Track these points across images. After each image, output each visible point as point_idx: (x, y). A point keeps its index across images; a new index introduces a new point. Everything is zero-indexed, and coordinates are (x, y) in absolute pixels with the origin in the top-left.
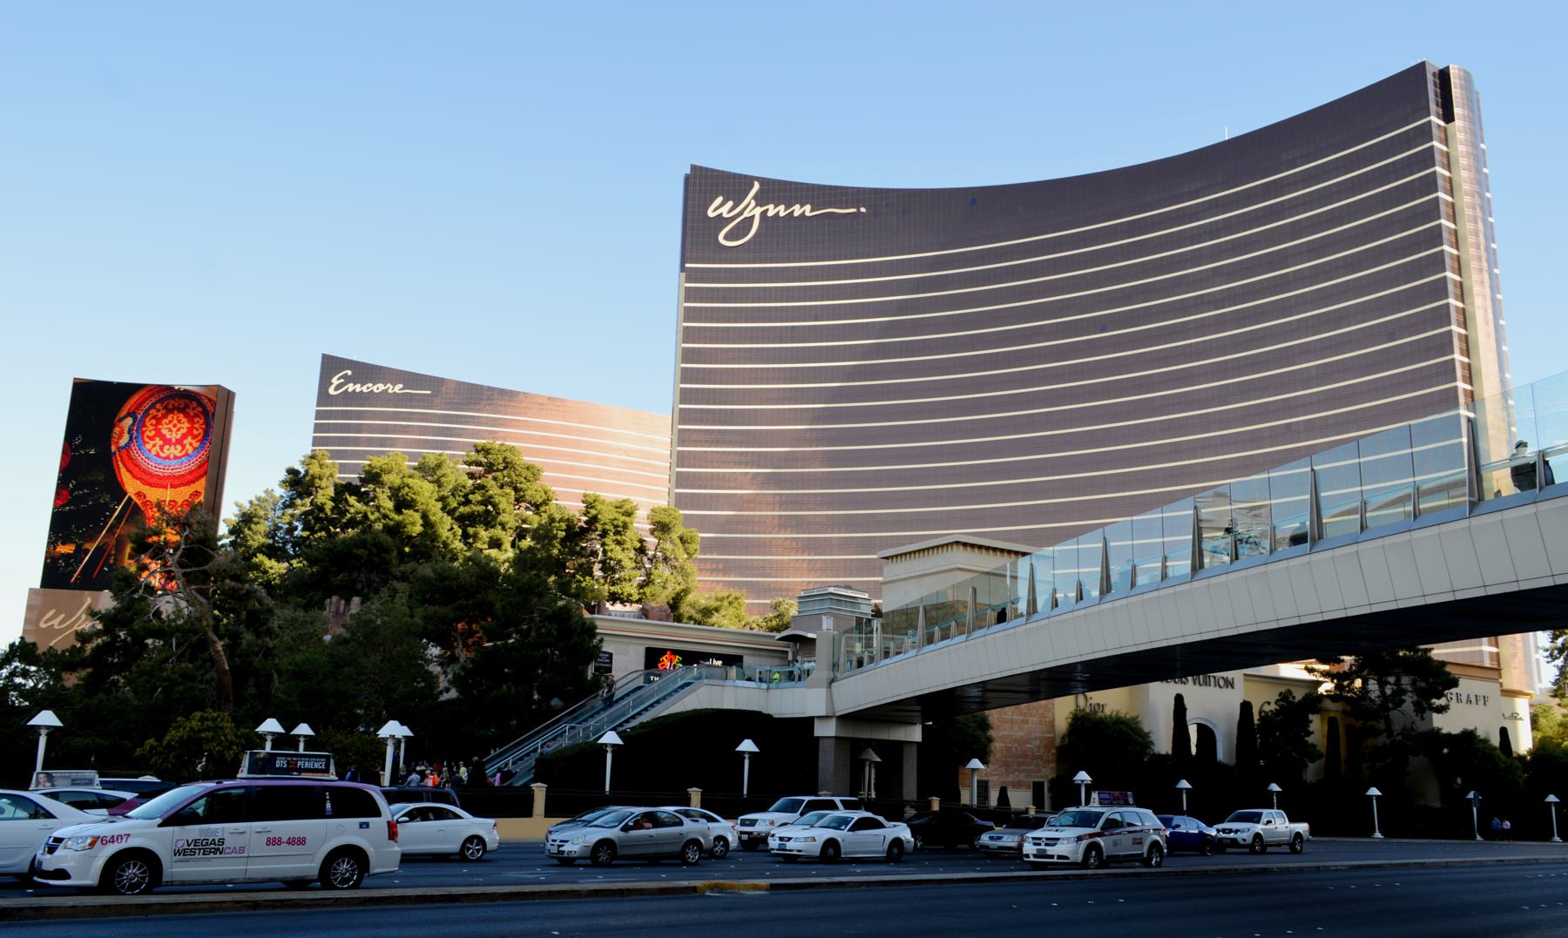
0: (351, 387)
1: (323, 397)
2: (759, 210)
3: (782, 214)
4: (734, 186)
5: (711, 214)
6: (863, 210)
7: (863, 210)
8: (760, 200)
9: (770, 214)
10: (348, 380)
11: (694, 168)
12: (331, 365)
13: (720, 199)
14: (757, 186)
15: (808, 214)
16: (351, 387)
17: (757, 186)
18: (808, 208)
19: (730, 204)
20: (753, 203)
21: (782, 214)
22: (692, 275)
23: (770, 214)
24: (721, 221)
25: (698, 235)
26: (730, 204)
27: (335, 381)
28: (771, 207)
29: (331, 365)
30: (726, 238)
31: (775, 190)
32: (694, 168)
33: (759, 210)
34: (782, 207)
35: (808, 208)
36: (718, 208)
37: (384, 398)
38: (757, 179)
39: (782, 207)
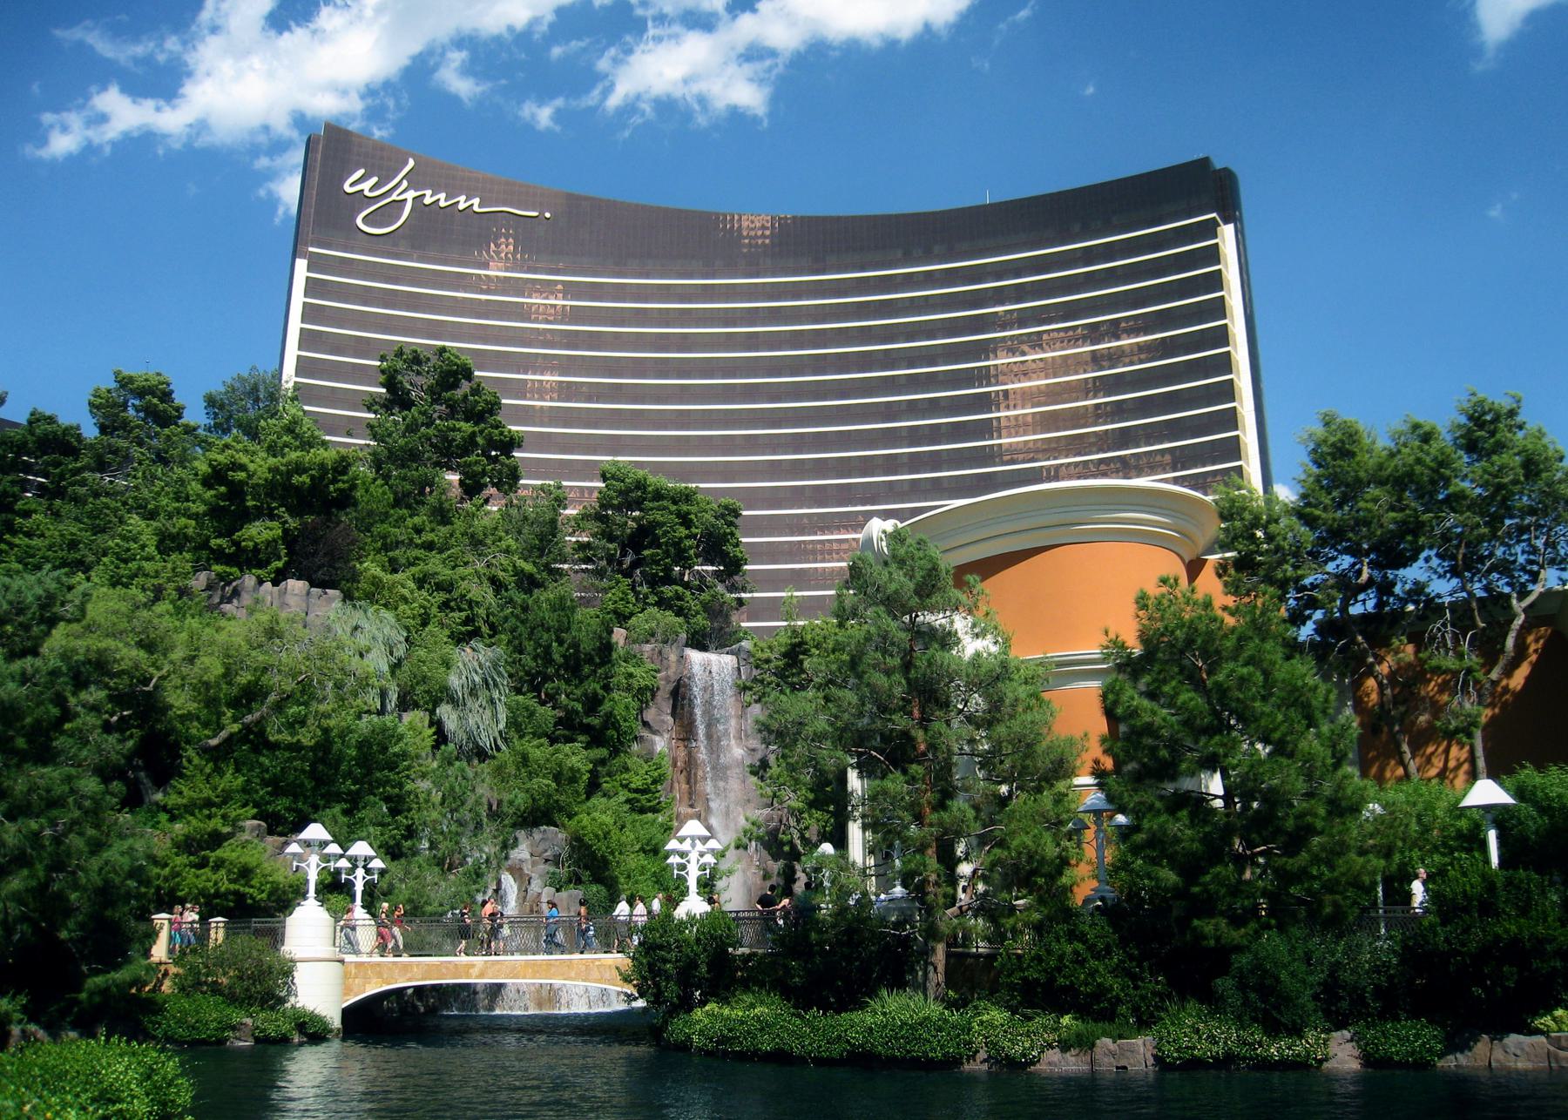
2: (411, 195)
3: (442, 204)
7: (548, 215)
8: (414, 180)
9: (428, 201)
13: (361, 172)
14: (411, 163)
15: (476, 208)
17: (411, 163)
18: (476, 201)
19: (374, 180)
20: (405, 184)
22: (315, 264)
24: (360, 199)
26: (374, 180)
33: (411, 195)
34: (442, 196)
35: (476, 201)
39: (442, 196)
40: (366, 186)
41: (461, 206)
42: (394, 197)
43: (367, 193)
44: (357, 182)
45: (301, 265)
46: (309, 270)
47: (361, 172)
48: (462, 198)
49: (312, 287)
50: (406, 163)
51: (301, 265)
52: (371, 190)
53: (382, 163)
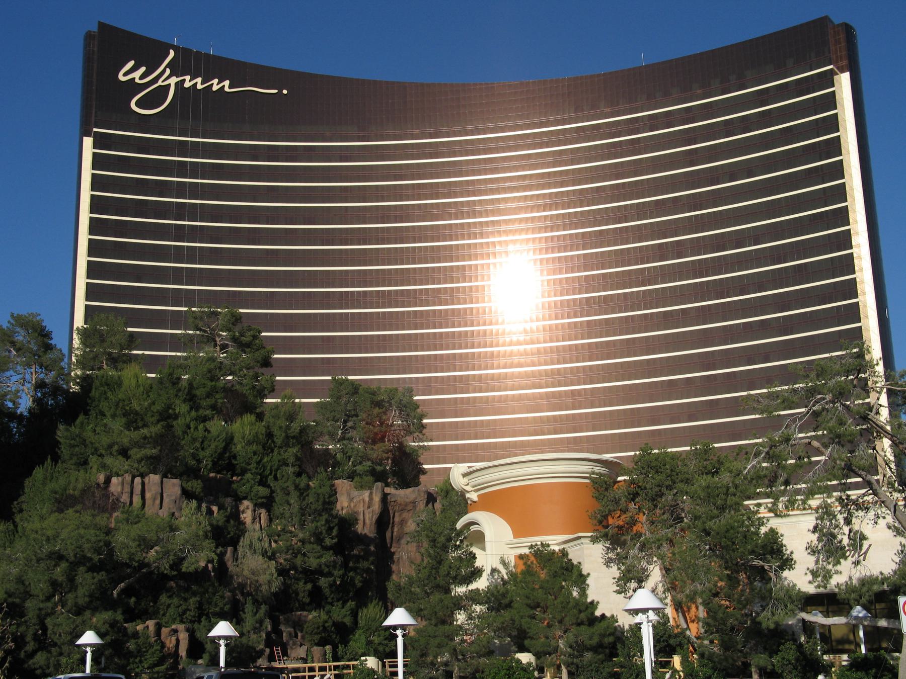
2: (173, 80)
3: (199, 87)
5: (121, 78)
6: (285, 92)
7: (285, 92)
9: (187, 85)
11: (102, 26)
13: (132, 63)
14: (172, 53)
15: (227, 89)
17: (172, 53)
18: (227, 83)
19: (143, 69)
21: (199, 87)
23: (187, 85)
24: (132, 87)
26: (143, 69)
28: (188, 78)
30: (138, 104)
32: (102, 26)
33: (173, 80)
34: (199, 80)
35: (227, 83)
36: (129, 73)
39: (199, 80)
40: (137, 75)
41: (215, 88)
42: (160, 83)
43: (137, 81)
44: (129, 73)
45: (88, 142)
46: (94, 148)
47: (132, 63)
48: (216, 81)
49: (98, 162)
50: (168, 54)
51: (88, 142)
52: (141, 78)
53: (149, 53)
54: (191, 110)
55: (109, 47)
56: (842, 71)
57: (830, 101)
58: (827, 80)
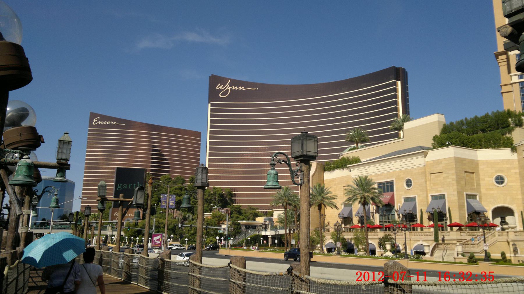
0: (100, 123)
1: (91, 125)
2: (230, 88)
4: (223, 81)
8: (231, 85)
10: (98, 120)
12: (93, 116)
16: (100, 123)
22: (212, 105)
24: (220, 91)
25: (213, 95)
27: (95, 121)
29: (93, 116)
31: (234, 83)
33: (230, 88)
36: (219, 87)
37: (110, 126)
38: (229, 79)
40: (221, 87)
44: (219, 87)
49: (212, 110)
53: (223, 81)
54: (235, 96)
55: (214, 80)
56: (399, 81)
57: (395, 90)
58: (395, 84)
